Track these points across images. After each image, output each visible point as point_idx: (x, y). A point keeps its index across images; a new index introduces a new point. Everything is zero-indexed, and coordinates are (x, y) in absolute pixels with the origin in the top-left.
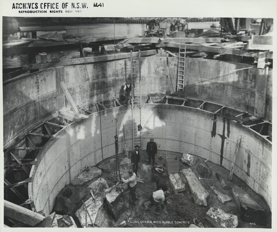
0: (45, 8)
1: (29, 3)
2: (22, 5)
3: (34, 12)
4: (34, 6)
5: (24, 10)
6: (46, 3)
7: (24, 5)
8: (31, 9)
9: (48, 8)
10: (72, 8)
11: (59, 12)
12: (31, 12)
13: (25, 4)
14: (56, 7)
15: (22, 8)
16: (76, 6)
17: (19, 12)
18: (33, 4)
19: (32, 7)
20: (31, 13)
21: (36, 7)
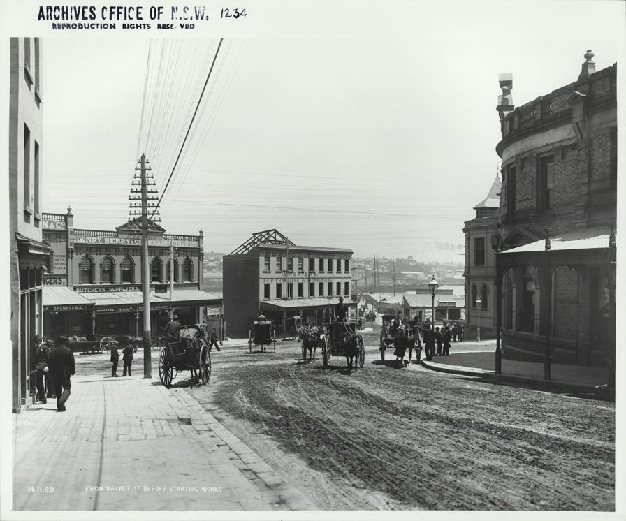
0: (111, 19)
1: (75, 8)
3: (87, 26)
4: (88, 13)
5: (65, 22)
6: (115, 8)
7: (65, 10)
8: (81, 21)
9: (118, 18)
10: (173, 19)
11: (142, 26)
12: (81, 26)
14: (137, 16)
17: (54, 26)
20: (79, 28)
21: (91, 16)
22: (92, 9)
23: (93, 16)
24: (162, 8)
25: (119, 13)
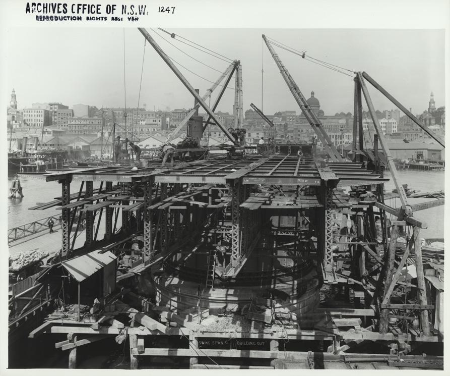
0: (78, 13)
2: (95, 7)
3: (61, 18)
5: (45, 15)
6: (81, 5)
7: (45, 6)
8: (56, 14)
9: (83, 13)
10: (122, 13)
11: (101, 19)
13: (47, 4)
15: (41, 11)
16: (128, 10)
17: (37, 17)
18: (59, 4)
19: (58, 10)
20: (56, 20)
21: (63, 10)
22: (65, 5)
23: (65, 11)
24: (115, 5)
25: (84, 9)
